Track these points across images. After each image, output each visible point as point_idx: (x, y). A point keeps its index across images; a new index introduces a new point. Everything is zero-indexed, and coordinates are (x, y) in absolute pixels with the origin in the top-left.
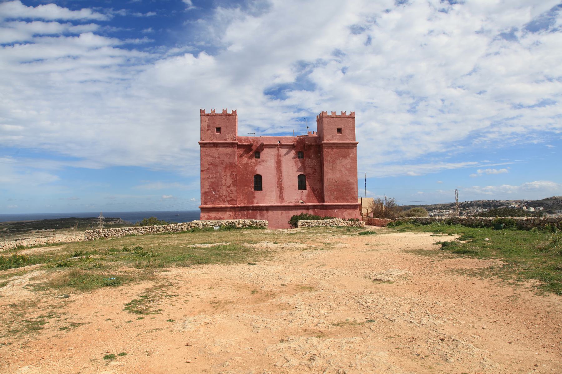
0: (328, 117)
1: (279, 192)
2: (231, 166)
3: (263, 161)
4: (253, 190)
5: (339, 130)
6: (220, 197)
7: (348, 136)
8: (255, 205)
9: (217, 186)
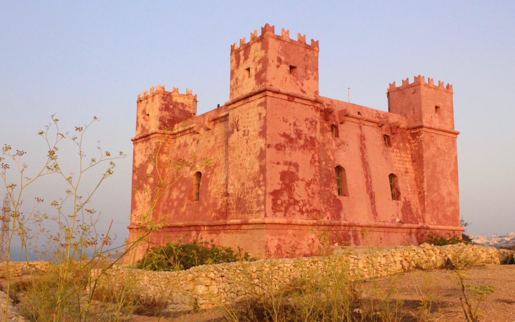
0: (425, 85)
1: (369, 201)
3: (343, 143)
4: (336, 194)
6: (296, 202)
8: (343, 222)
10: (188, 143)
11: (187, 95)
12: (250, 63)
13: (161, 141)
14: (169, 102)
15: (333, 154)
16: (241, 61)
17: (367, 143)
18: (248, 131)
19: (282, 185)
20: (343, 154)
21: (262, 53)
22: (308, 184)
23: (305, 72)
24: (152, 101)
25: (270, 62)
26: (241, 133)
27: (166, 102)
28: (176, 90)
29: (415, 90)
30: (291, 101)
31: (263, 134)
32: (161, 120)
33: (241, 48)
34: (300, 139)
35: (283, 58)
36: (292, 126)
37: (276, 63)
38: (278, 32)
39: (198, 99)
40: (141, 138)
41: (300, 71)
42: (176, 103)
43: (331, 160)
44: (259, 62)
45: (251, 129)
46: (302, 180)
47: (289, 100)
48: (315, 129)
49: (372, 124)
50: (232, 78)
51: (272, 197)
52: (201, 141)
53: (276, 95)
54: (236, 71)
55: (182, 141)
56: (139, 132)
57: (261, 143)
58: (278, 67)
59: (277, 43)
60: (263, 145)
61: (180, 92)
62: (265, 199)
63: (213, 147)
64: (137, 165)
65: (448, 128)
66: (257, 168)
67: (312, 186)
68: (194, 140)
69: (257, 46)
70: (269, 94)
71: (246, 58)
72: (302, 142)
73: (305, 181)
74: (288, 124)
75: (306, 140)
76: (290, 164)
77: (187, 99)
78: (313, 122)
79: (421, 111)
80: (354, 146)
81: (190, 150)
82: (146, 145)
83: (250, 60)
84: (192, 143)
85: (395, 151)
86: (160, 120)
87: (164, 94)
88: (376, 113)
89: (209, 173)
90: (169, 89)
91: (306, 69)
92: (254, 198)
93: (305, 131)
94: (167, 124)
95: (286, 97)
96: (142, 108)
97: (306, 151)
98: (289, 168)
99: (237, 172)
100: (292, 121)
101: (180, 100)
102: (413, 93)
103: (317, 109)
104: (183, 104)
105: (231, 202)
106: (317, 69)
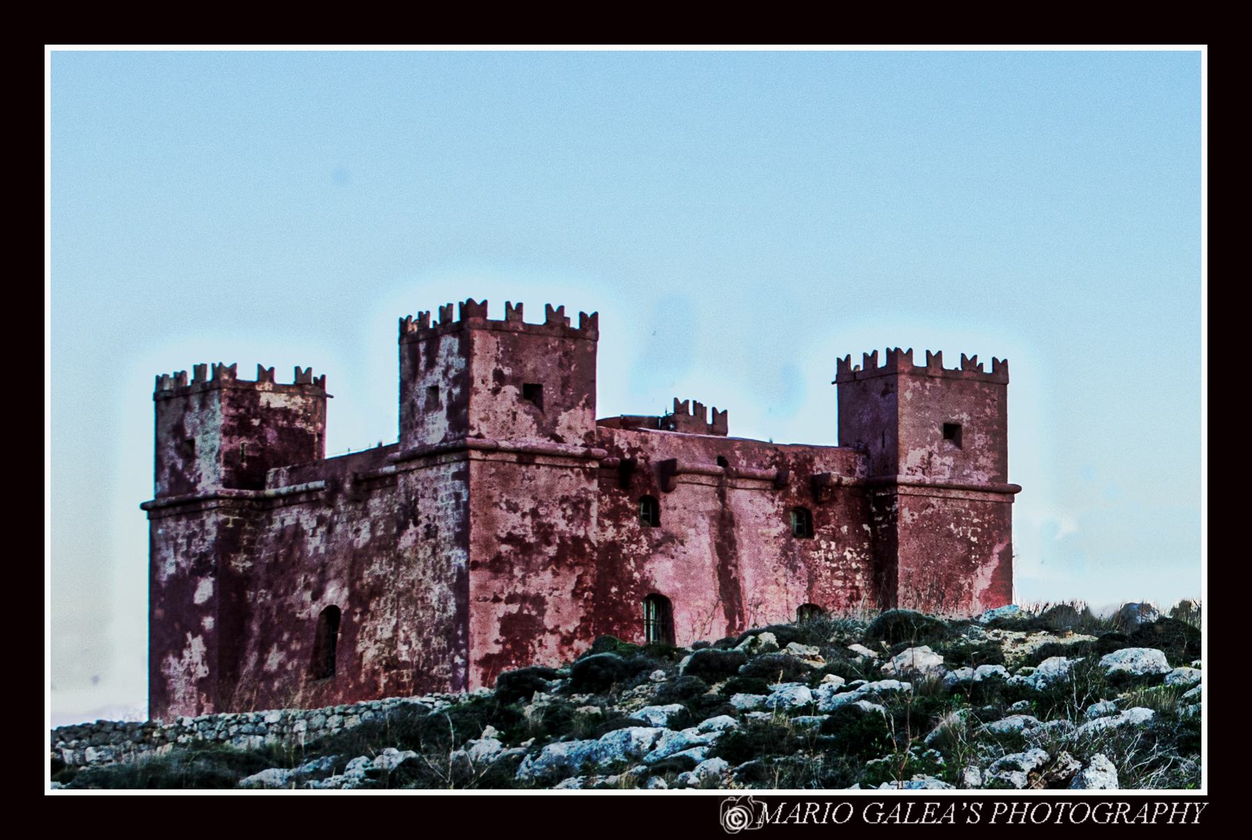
0: (916, 373)
2: (572, 551)
3: (670, 538)
5: (952, 432)
9: (530, 635)
10: (305, 527)
11: (296, 385)
12: (436, 376)
13: (231, 518)
14: (248, 410)
15: (639, 568)
16: (422, 368)
18: (436, 527)
19: (504, 643)
21: (459, 363)
22: (567, 641)
23: (562, 393)
24: (203, 406)
25: (477, 383)
26: (421, 529)
27: (242, 410)
28: (266, 375)
29: (887, 384)
30: (527, 464)
31: (462, 540)
32: (230, 459)
33: (421, 337)
34: (549, 544)
35: (507, 371)
38: (496, 313)
39: (329, 390)
40: (171, 505)
41: (550, 393)
42: (268, 409)
44: (455, 381)
45: (441, 524)
46: (553, 632)
47: (520, 462)
48: (587, 518)
49: (757, 484)
51: (481, 670)
52: (339, 528)
53: (491, 457)
54: (411, 385)
55: (289, 521)
57: (458, 557)
58: (496, 391)
59: (493, 341)
60: (463, 562)
61: (279, 380)
62: (467, 675)
63: (366, 546)
66: (452, 609)
67: (577, 644)
68: (321, 521)
69: (449, 343)
70: (475, 455)
71: (431, 364)
72: (551, 551)
73: (560, 633)
74: (519, 514)
75: (562, 546)
76: (524, 598)
78: (579, 507)
79: (896, 442)
81: (310, 548)
82: (188, 527)
83: (438, 370)
84: (314, 530)
85: (824, 546)
86: (226, 463)
87: (235, 390)
88: (770, 453)
89: (358, 610)
90: (247, 373)
92: (448, 672)
93: (562, 525)
94: (245, 472)
95: (514, 458)
96: (171, 422)
97: (564, 571)
98: (521, 609)
99: (415, 614)
100: (528, 505)
101: (278, 401)
103: (590, 475)
104: (285, 412)
105: (405, 679)
106: (594, 381)
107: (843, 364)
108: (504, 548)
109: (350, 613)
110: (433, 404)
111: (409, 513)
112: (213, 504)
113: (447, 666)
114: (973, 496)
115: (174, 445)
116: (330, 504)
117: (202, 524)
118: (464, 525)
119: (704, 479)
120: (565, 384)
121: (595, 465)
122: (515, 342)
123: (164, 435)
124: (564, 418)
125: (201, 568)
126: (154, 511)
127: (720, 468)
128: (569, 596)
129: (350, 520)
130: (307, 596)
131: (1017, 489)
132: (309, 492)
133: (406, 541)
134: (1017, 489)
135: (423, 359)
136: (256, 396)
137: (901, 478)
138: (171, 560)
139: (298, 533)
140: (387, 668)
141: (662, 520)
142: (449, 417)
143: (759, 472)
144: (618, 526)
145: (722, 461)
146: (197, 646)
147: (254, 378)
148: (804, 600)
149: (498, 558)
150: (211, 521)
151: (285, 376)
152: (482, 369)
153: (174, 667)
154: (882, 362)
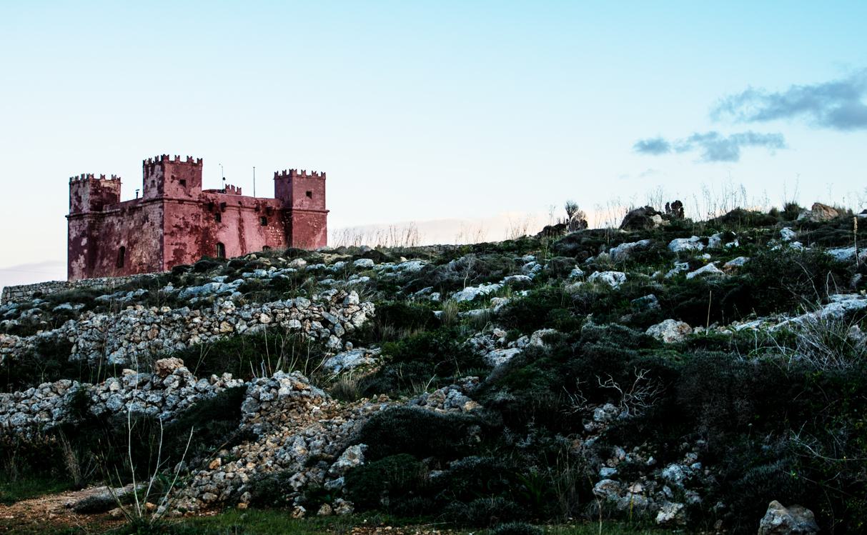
0: (298, 176)
2: (195, 230)
3: (224, 226)
5: (309, 194)
7: (318, 203)
11: (112, 180)
12: (154, 177)
15: (215, 235)
16: (150, 175)
17: (245, 225)
20: (224, 234)
21: (161, 173)
22: (193, 257)
24: (84, 186)
25: (166, 180)
28: (103, 177)
31: (162, 226)
36: (181, 220)
37: (171, 180)
38: (172, 158)
39: (121, 182)
40: (74, 216)
41: (188, 183)
43: (213, 239)
44: (160, 179)
45: (155, 222)
47: (179, 203)
48: (199, 220)
50: (144, 184)
52: (125, 223)
56: (72, 210)
57: (161, 232)
58: (172, 182)
59: (171, 167)
64: (72, 238)
65: (318, 208)
66: (159, 247)
68: (119, 221)
69: (158, 167)
70: (166, 201)
71: (152, 174)
72: (189, 230)
75: (192, 228)
76: (180, 244)
77: (113, 184)
78: (197, 216)
79: (292, 197)
80: (233, 228)
83: (154, 176)
86: (91, 203)
90: (97, 177)
91: (193, 179)
93: (192, 222)
94: (97, 206)
95: (177, 202)
96: (74, 191)
97: (192, 236)
100: (181, 216)
102: (289, 182)
103: (200, 207)
104: (109, 188)
107: (276, 174)
108: (175, 229)
109: (128, 248)
110: (153, 186)
111: (146, 218)
112: (86, 216)
113: (157, 264)
114: (315, 213)
115: (75, 198)
116: (122, 215)
117: (83, 222)
118: (163, 222)
119: (234, 208)
120: (193, 179)
121: (202, 204)
122: (178, 167)
123: (72, 195)
124: (192, 190)
125: (83, 235)
126: (69, 218)
127: (239, 205)
128: (193, 243)
129: (128, 220)
130: (115, 243)
131: (329, 211)
132: (116, 212)
133: (145, 227)
134: (329, 211)
135: (150, 172)
136: (100, 183)
137: (293, 208)
138: (74, 233)
139: (112, 224)
140: (139, 265)
141: (222, 220)
142: (158, 189)
143: (251, 206)
144: (208, 222)
145: (240, 203)
146: (82, 258)
147: (99, 178)
148: (265, 244)
149: (173, 232)
150: (86, 221)
151: (108, 177)
152: (168, 175)
153: (75, 264)
154: (288, 173)
